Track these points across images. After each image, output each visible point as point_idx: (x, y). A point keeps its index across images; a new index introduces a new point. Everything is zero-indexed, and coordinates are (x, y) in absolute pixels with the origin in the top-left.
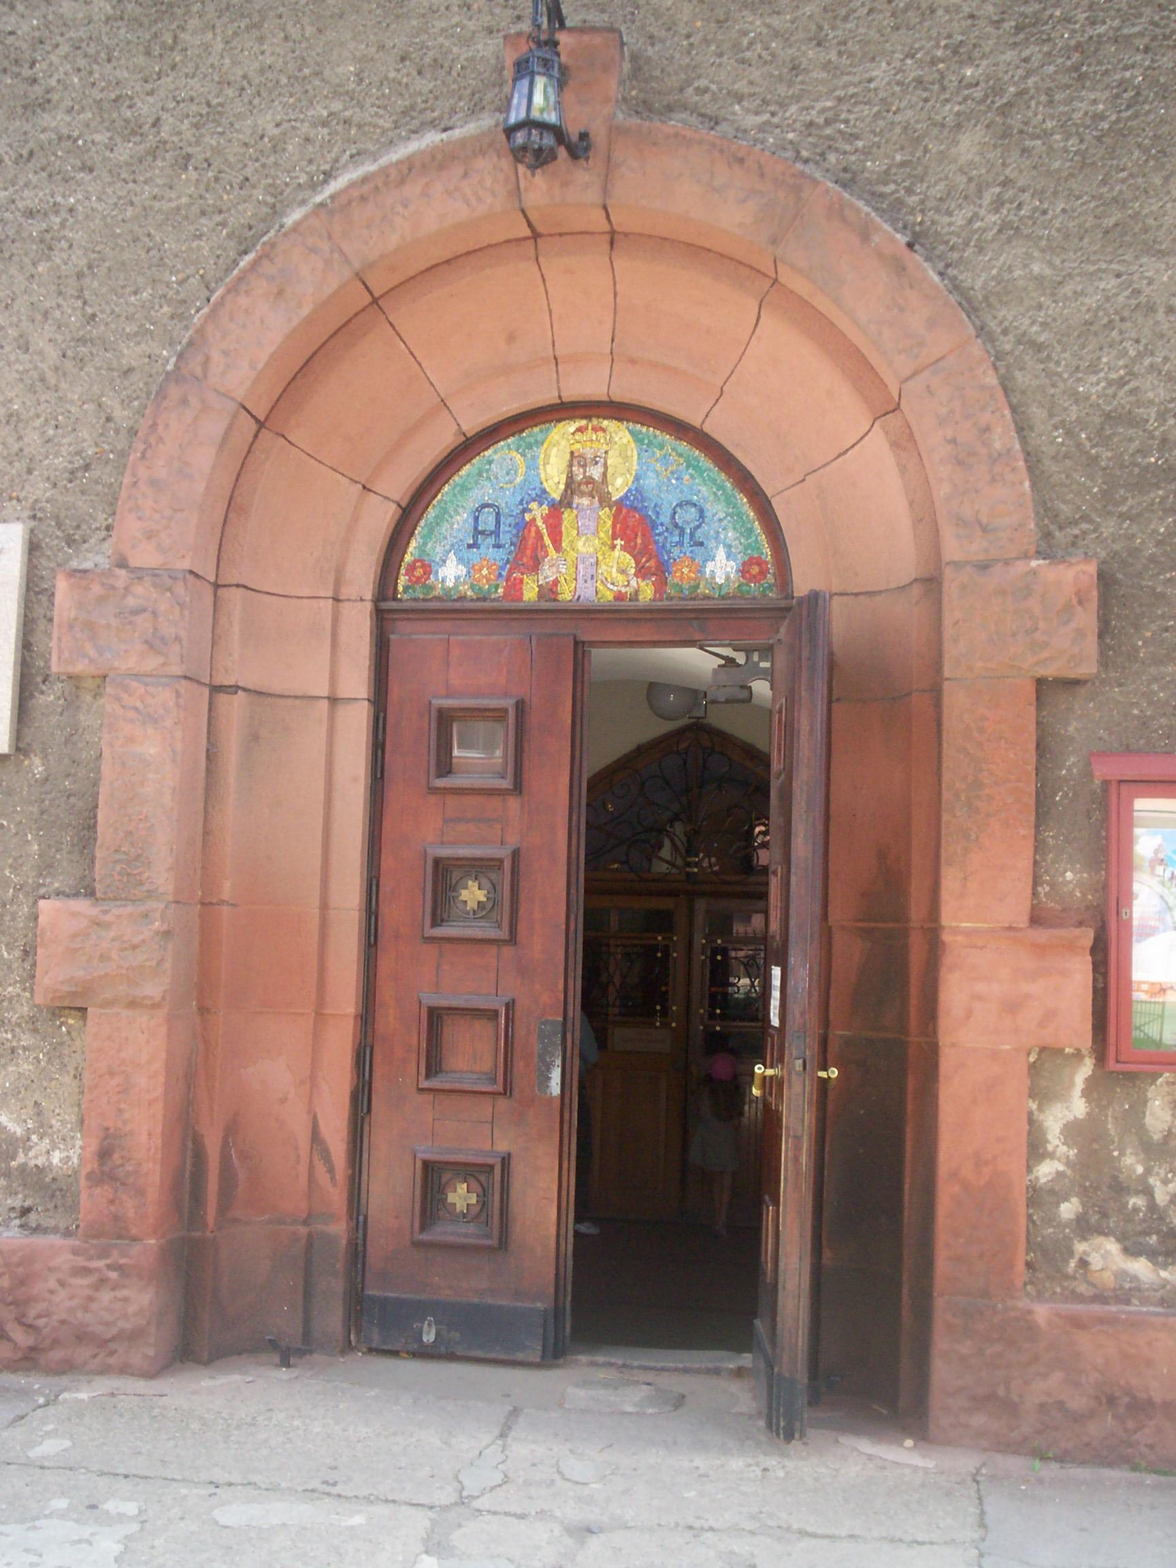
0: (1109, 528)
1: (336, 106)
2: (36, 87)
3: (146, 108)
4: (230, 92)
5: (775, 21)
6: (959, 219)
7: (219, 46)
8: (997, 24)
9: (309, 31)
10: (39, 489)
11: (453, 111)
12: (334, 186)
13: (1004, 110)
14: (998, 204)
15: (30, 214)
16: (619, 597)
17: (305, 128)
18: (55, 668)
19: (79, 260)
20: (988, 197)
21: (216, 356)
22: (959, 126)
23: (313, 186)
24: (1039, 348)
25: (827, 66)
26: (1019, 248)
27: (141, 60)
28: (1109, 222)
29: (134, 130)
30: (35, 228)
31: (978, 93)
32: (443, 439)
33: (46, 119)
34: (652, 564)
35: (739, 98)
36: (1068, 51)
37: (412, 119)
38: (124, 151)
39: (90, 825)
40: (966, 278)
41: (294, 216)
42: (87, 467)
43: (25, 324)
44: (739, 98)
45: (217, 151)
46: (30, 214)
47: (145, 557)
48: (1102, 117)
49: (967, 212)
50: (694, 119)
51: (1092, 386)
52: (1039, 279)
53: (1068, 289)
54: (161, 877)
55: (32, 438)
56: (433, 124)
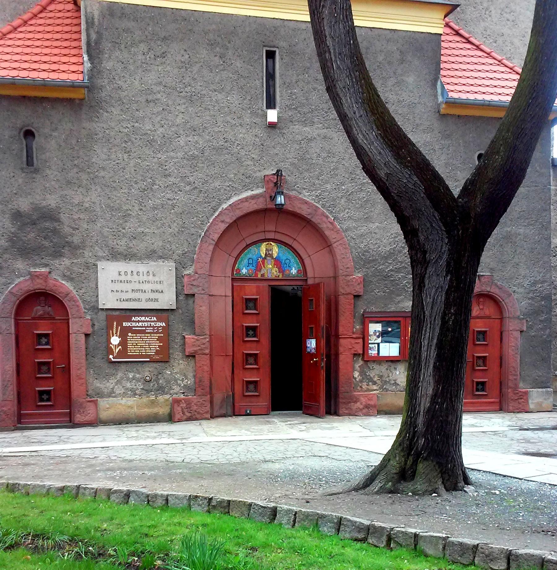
1: (230, 183)
2: (166, 172)
3: (191, 179)
4: (209, 178)
5: (310, 174)
8: (348, 179)
9: (224, 166)
10: (175, 257)
11: (253, 187)
14: (348, 212)
15: (169, 199)
17: (225, 187)
19: (180, 210)
20: (346, 212)
24: (354, 239)
26: (351, 221)
27: (190, 169)
30: (170, 202)
33: (170, 179)
35: (305, 189)
36: (360, 185)
37: (246, 188)
38: (188, 188)
41: (225, 206)
42: (185, 253)
43: (170, 223)
44: (305, 189)
45: (207, 190)
46: (169, 199)
48: (364, 198)
50: (297, 193)
51: (362, 246)
52: (354, 227)
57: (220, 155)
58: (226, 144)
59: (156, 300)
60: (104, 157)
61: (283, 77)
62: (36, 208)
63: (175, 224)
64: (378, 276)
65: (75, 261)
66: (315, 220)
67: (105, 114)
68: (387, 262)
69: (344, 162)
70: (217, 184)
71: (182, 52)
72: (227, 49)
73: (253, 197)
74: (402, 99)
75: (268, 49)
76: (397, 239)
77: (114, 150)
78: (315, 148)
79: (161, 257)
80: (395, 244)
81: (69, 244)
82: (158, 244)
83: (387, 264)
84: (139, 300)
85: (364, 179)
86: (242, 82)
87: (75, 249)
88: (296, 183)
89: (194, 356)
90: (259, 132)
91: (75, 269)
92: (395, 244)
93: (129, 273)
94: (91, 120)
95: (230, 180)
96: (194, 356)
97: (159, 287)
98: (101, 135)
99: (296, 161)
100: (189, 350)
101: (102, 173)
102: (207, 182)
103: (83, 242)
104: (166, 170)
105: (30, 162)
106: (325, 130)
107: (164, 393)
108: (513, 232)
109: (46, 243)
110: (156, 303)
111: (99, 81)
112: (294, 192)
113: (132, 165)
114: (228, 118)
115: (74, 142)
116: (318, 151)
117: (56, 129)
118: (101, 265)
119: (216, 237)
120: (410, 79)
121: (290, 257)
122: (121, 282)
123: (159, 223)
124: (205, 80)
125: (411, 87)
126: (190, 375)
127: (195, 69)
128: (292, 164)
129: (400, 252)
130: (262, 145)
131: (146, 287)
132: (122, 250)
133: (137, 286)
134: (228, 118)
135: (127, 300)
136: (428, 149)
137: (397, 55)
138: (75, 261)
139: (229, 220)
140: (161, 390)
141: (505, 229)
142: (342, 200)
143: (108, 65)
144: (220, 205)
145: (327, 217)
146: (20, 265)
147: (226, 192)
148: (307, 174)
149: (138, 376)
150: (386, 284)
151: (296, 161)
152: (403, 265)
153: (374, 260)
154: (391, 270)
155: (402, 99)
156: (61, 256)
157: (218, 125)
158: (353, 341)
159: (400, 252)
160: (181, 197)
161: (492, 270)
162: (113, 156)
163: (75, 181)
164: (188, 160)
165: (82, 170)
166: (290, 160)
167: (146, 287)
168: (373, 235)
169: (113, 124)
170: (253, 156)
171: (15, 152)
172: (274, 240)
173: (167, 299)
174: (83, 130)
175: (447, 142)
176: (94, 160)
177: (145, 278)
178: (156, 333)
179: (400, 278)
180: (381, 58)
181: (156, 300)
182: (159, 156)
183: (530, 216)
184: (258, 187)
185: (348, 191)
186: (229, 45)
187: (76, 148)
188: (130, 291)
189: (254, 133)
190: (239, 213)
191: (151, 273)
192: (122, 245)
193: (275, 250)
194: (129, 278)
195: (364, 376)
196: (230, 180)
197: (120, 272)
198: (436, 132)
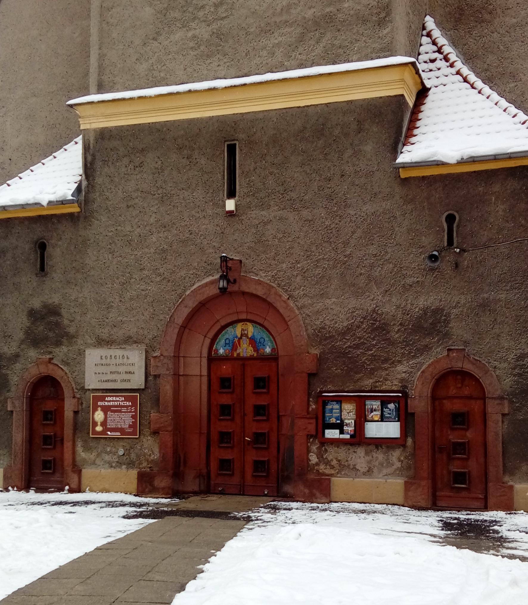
0: (321, 347)
6: (297, 292)
10: (147, 341)
12: (195, 287)
13: (304, 273)
15: (143, 290)
18: (152, 374)
20: (301, 289)
21: (176, 318)
22: (297, 276)
23: (191, 286)
24: (309, 316)
25: (276, 264)
26: (306, 299)
28: (321, 293)
31: (300, 269)
35: (261, 270)
37: (208, 274)
39: (158, 400)
40: (297, 304)
41: (188, 292)
44: (261, 270)
47: (165, 354)
48: (319, 274)
49: (298, 292)
51: (318, 323)
52: (310, 304)
53: (314, 305)
55: (146, 332)
58: (191, 236)
61: (242, 167)
62: (45, 306)
63: (147, 312)
64: (335, 353)
65: (71, 348)
66: (271, 299)
67: (96, 222)
68: (345, 338)
69: (299, 240)
70: (183, 273)
71: (156, 159)
72: (193, 150)
73: (212, 282)
74: (359, 169)
75: (229, 143)
76: (355, 314)
79: (136, 342)
80: (353, 319)
81: (67, 334)
82: (132, 330)
83: (344, 340)
84: (115, 381)
85: (319, 255)
86: (206, 177)
87: (71, 337)
88: (254, 265)
89: (158, 433)
91: (70, 355)
92: (353, 319)
93: (109, 357)
95: (195, 268)
97: (131, 369)
98: (92, 240)
99: (253, 245)
101: (92, 273)
102: (174, 272)
103: (77, 332)
104: (141, 264)
105: (42, 268)
106: (280, 212)
108: (491, 298)
109: (51, 334)
110: (128, 383)
111: (93, 195)
112: (251, 274)
113: (114, 263)
114: (193, 212)
116: (273, 232)
118: (87, 352)
119: (180, 320)
120: (368, 148)
121: (265, 336)
122: (102, 365)
124: (174, 180)
125: (369, 156)
127: (166, 172)
128: (249, 248)
129: (358, 327)
131: (121, 369)
132: (105, 338)
133: (114, 369)
135: (106, 381)
136: (388, 216)
137: (354, 126)
138: (71, 348)
139: (192, 304)
141: (481, 296)
142: (298, 278)
143: (99, 180)
145: (280, 296)
146: (32, 353)
147: (190, 279)
148: (264, 256)
150: (344, 361)
151: (253, 245)
152: (362, 340)
153: (330, 337)
154: (350, 347)
155: (359, 169)
156: (61, 344)
158: (307, 421)
159: (358, 327)
162: (101, 258)
163: (73, 281)
165: (78, 271)
166: (248, 244)
167: (121, 369)
168: (330, 310)
171: (32, 261)
175: (410, 207)
176: (86, 262)
177: (121, 361)
178: (130, 412)
179: (358, 355)
180: (337, 132)
181: (129, 381)
182: (136, 253)
183: (513, 279)
184: (218, 272)
185: (303, 269)
186: (195, 146)
188: (109, 373)
190: (201, 298)
191: (126, 356)
192: (105, 333)
193: (251, 329)
194: (108, 361)
195: (321, 459)
197: (101, 357)
198: (397, 197)
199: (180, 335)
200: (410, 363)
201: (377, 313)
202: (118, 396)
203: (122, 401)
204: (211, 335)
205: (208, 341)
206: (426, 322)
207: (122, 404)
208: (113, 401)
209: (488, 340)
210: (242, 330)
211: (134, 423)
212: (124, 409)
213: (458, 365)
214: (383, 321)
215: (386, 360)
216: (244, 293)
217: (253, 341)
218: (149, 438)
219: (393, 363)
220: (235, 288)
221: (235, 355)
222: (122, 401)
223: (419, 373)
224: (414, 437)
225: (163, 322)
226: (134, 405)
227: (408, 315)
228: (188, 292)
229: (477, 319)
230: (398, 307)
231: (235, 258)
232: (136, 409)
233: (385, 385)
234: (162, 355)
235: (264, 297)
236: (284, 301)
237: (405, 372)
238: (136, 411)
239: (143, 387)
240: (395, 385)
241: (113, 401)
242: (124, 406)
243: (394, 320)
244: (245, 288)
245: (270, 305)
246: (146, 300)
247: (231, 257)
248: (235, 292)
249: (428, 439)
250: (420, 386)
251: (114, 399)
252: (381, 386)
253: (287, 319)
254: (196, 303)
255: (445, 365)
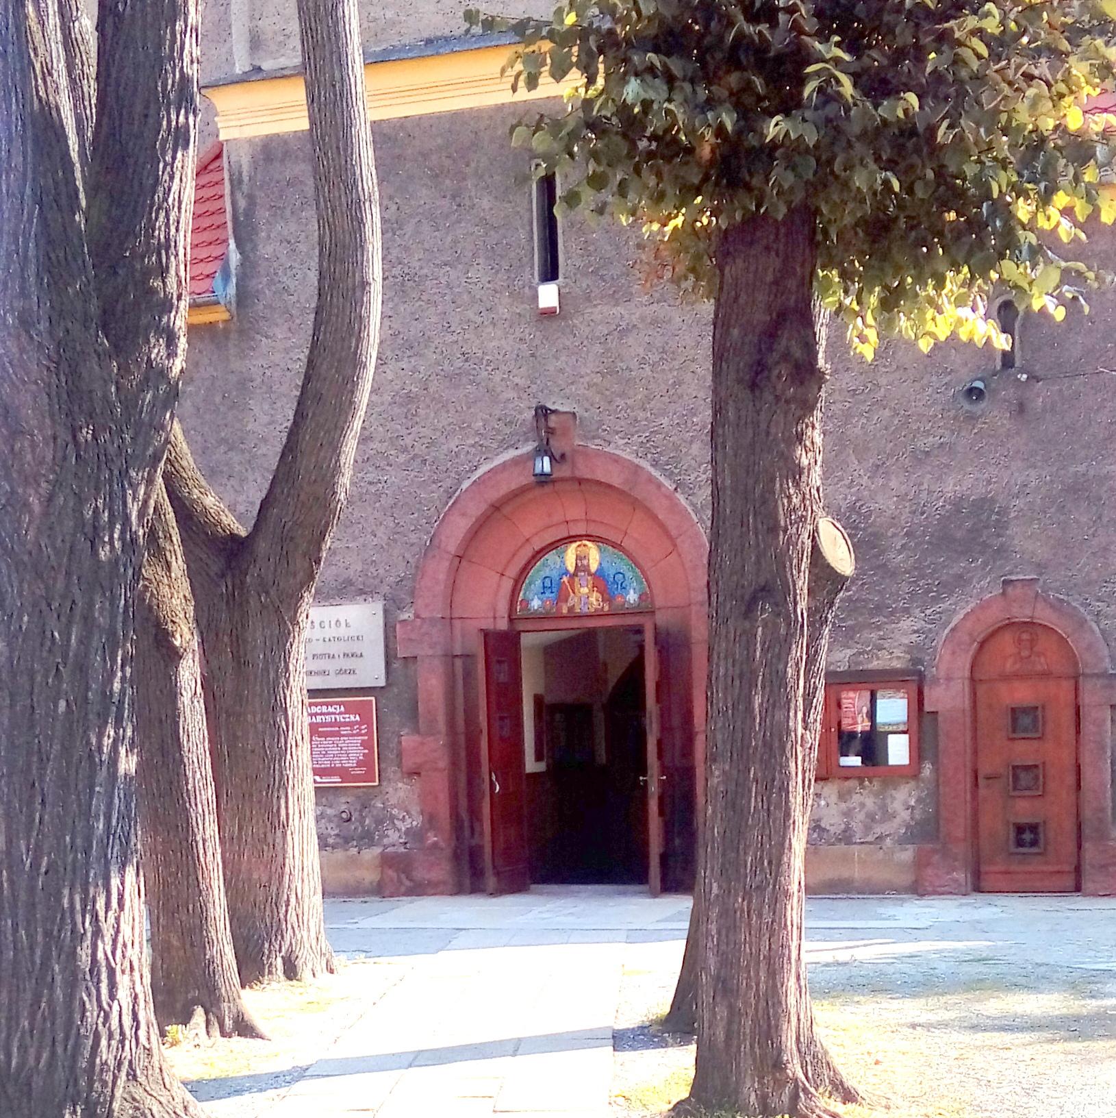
3: (408, 441)
7: (432, 415)
10: (385, 589)
15: (370, 483)
16: (596, 610)
17: (466, 448)
19: (391, 501)
21: (443, 538)
29: (405, 450)
30: (373, 489)
32: (527, 553)
33: (372, 445)
34: (607, 596)
37: (505, 445)
38: (402, 458)
39: (415, 708)
40: (695, 501)
41: (466, 485)
46: (370, 483)
54: (441, 725)
56: (512, 446)
57: (457, 387)
59: (352, 672)
60: (266, 419)
66: (638, 493)
73: (516, 462)
77: (279, 404)
78: (635, 346)
79: (361, 592)
88: (601, 423)
90: (527, 331)
94: (242, 356)
95: (478, 433)
96: (418, 774)
97: (355, 647)
99: (598, 379)
100: (409, 763)
102: (432, 443)
107: (372, 844)
110: (352, 676)
112: (597, 441)
115: (218, 399)
117: (192, 380)
123: (356, 529)
126: (415, 810)
130: (533, 355)
134: (470, 314)
140: (367, 838)
144: (459, 482)
147: (470, 457)
149: (329, 811)
157: (452, 329)
160: (393, 477)
161: (1041, 567)
164: (401, 405)
166: (587, 379)
167: (334, 648)
169: (277, 357)
170: (517, 380)
172: (589, 537)
173: (372, 672)
174: (230, 377)
181: (352, 672)
184: (527, 440)
187: (222, 409)
189: (518, 334)
190: (494, 495)
193: (594, 556)
196: (478, 433)
199: (455, 572)
200: (928, 612)
201: (859, 514)
202: (331, 704)
203: (340, 713)
204: (513, 571)
205: (508, 584)
206: (960, 527)
207: (340, 718)
208: (321, 714)
209: (1085, 559)
210: (578, 558)
211: (368, 757)
212: (345, 730)
213: (1021, 613)
214: (870, 530)
215: (878, 609)
216: (580, 481)
217: (600, 581)
218: (400, 785)
219: (892, 613)
220: (564, 471)
221: (565, 611)
222: (340, 713)
223: (946, 631)
224: (935, 763)
225: (416, 549)
226: (365, 720)
227: (922, 514)
228: (466, 485)
229: (1062, 518)
230: (901, 498)
231: (561, 409)
232: (370, 727)
233: (878, 659)
234: (417, 616)
235: (626, 489)
236: (666, 496)
237: (915, 632)
238: (369, 733)
239: (382, 683)
240: (899, 658)
241: (321, 714)
242: (345, 724)
243: (894, 525)
244: (583, 471)
245: (636, 504)
246: (378, 505)
247: (553, 408)
248: (562, 480)
249: (965, 766)
250: (947, 657)
251: (324, 709)
252: (869, 661)
253: (674, 533)
254: (484, 507)
255: (995, 615)
